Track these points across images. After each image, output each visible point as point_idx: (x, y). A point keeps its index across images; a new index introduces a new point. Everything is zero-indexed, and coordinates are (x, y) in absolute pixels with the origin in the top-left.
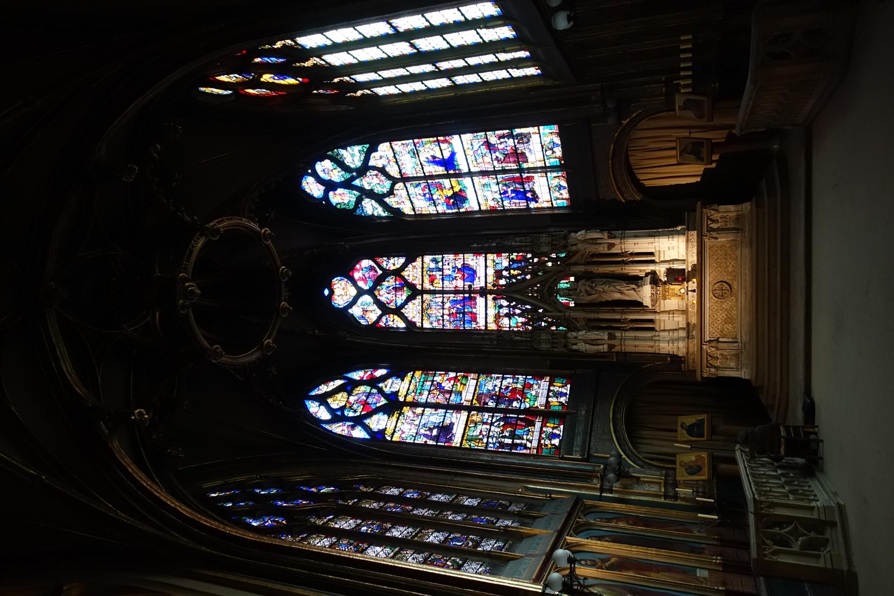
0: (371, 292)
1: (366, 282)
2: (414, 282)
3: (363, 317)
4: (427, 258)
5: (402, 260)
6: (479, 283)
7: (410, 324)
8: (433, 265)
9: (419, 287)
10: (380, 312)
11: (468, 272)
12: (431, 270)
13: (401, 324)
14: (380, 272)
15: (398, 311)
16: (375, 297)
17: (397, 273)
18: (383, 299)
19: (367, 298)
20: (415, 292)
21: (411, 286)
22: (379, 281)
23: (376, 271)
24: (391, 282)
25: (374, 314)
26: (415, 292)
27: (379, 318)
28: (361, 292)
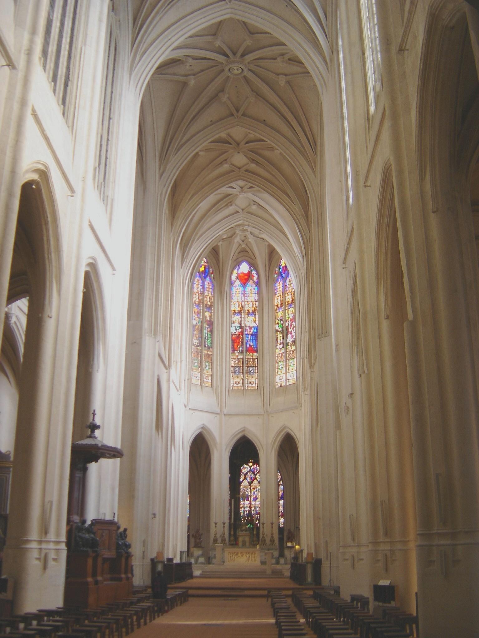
0: (250, 470)
1: (253, 468)
2: (253, 483)
3: (243, 467)
4: (259, 487)
5: (259, 480)
6: (253, 503)
7: (242, 482)
8: (257, 489)
9: (252, 485)
10: (245, 473)
11: (256, 499)
12: (256, 488)
13: (241, 480)
14: (256, 473)
15: (245, 478)
16: (249, 471)
17: (255, 478)
18: (249, 474)
19: (249, 469)
20: (250, 483)
21: (252, 482)
22: (253, 472)
23: (256, 471)
24: (253, 476)
25: (244, 471)
26: (250, 483)
27: (243, 473)
28: (250, 467)
